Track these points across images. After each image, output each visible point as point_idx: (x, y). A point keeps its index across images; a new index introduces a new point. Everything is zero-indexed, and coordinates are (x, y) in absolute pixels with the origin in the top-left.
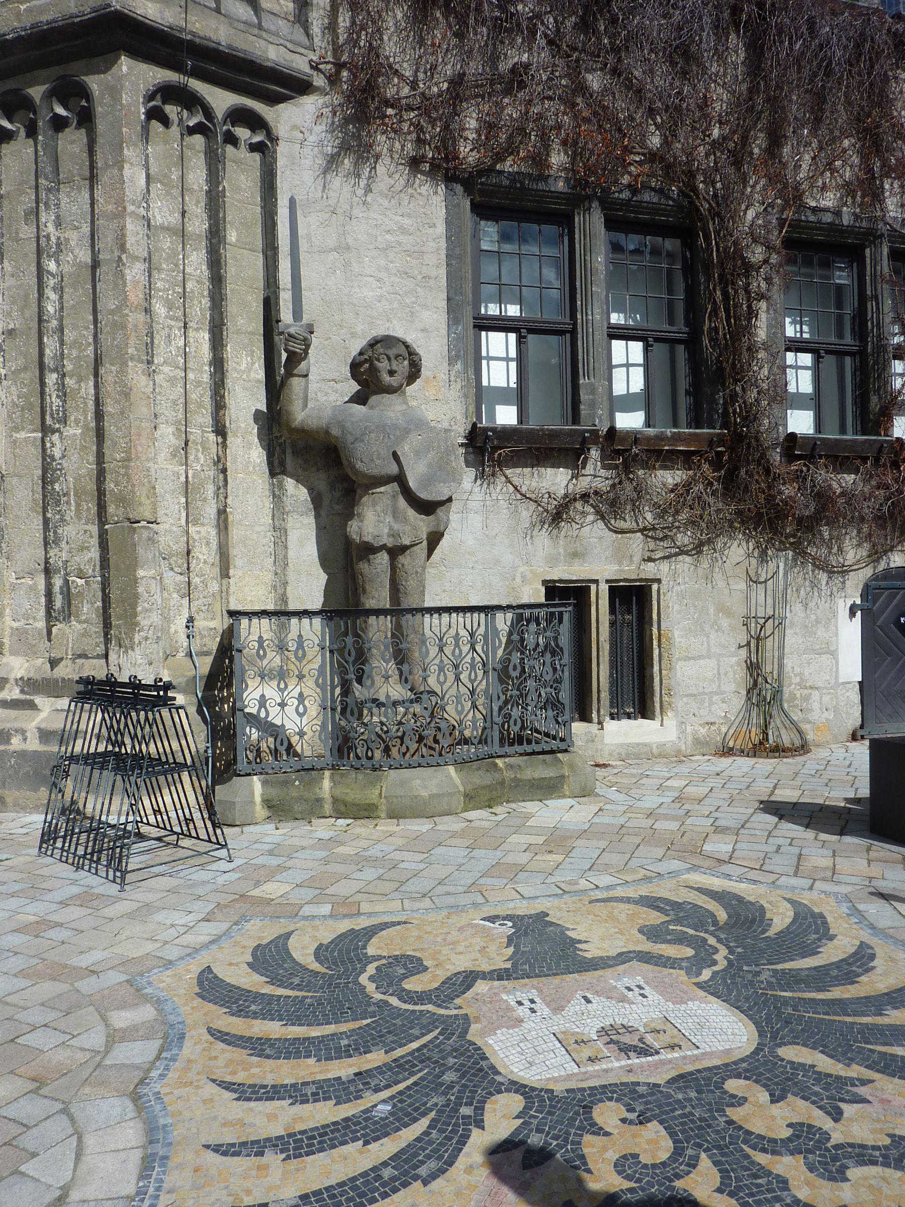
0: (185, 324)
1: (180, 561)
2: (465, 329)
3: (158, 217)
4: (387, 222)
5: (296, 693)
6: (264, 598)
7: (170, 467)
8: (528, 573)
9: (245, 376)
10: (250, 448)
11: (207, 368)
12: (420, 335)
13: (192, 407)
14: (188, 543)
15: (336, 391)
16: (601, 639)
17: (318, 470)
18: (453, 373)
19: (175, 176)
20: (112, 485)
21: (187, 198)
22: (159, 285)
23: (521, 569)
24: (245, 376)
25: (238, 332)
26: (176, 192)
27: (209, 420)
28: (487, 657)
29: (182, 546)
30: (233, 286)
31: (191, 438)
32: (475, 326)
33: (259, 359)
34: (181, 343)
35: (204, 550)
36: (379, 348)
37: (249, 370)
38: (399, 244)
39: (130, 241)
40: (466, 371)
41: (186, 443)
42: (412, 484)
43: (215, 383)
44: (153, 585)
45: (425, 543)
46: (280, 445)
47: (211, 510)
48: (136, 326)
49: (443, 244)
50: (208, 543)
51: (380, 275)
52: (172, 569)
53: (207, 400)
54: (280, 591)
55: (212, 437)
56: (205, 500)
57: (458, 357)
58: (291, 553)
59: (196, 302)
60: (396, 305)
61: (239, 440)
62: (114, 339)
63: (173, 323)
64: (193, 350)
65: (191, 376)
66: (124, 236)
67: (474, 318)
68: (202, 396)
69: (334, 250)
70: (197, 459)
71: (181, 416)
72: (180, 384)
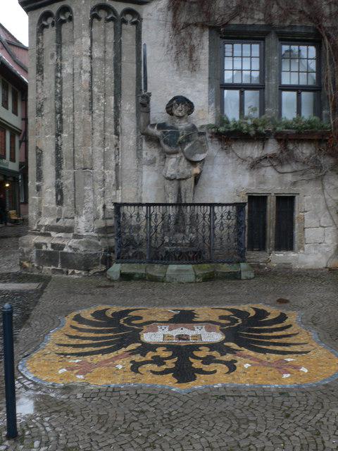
12: (197, 93)
19: (102, 38)
26: (102, 45)
27: (113, 130)
39: (84, 65)
47: (113, 164)
53: (112, 122)
55: (114, 136)
58: (144, 181)
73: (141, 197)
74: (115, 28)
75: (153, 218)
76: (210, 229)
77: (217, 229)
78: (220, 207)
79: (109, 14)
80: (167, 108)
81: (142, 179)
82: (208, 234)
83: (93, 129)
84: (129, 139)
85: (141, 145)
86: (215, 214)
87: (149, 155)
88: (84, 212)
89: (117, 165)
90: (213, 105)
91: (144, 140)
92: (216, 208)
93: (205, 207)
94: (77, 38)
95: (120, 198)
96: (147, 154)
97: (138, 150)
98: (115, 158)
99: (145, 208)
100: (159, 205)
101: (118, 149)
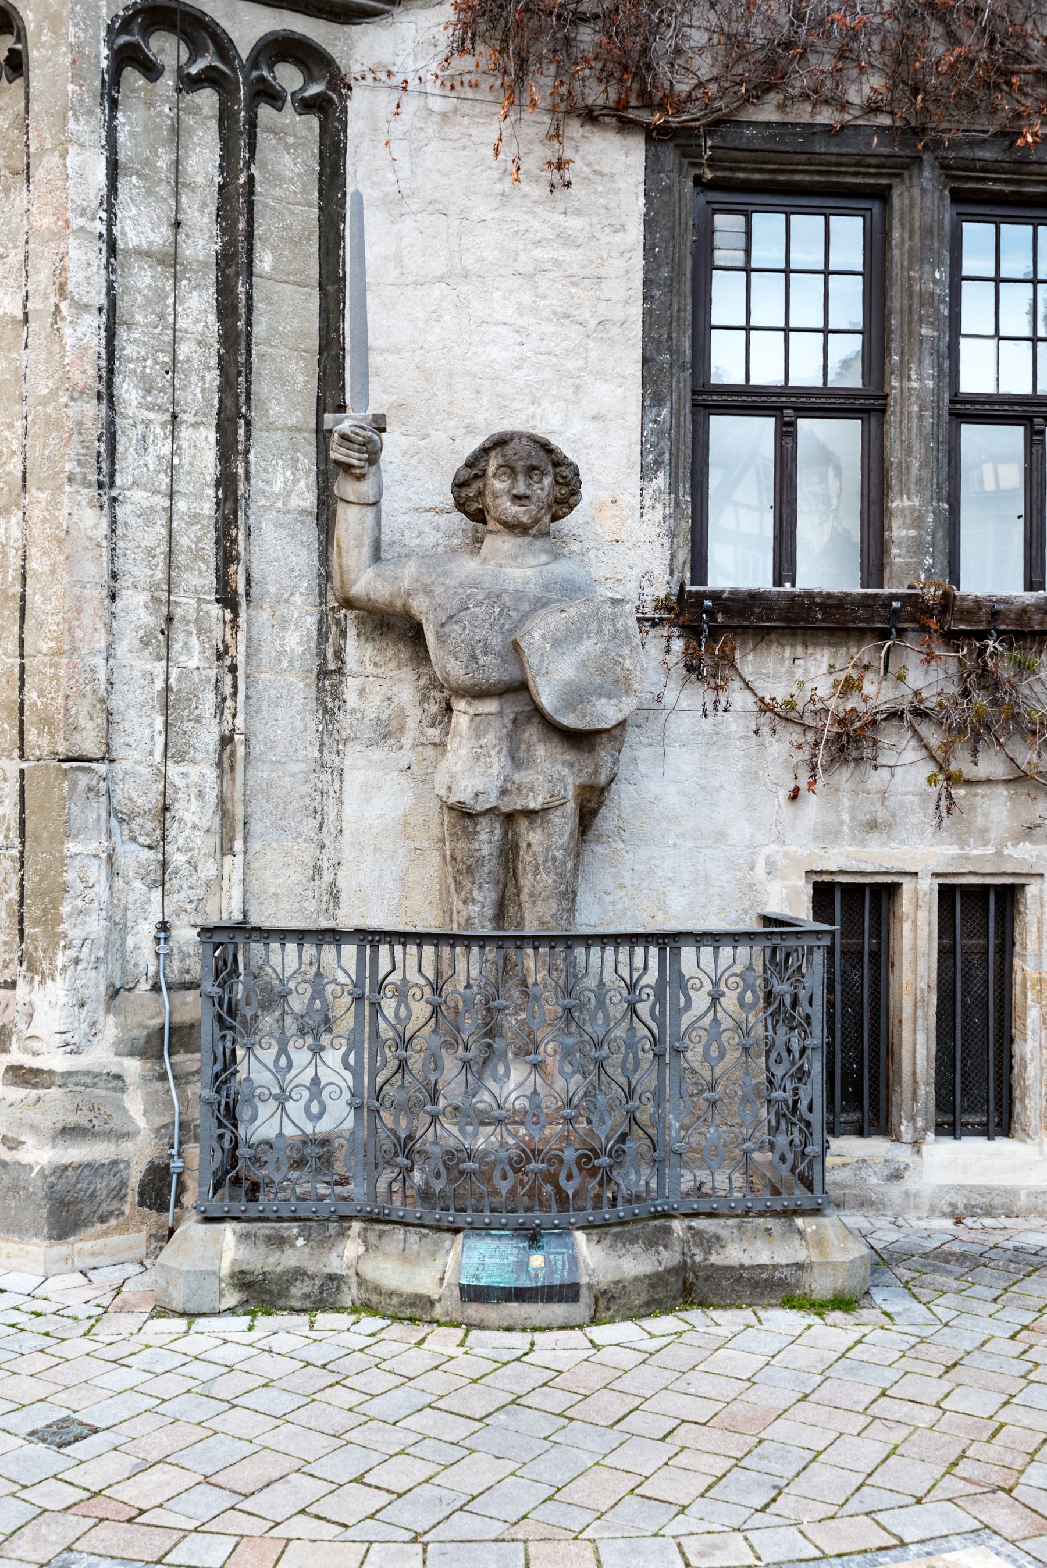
0: (174, 417)
1: (149, 826)
3: (131, 234)
4: (536, 224)
5: (307, 1077)
6: (299, 890)
7: (137, 664)
8: (779, 858)
9: (279, 504)
10: (284, 629)
11: (211, 492)
12: (590, 426)
13: (181, 559)
17: (399, 667)
18: (648, 493)
19: (163, 162)
20: (34, 695)
21: (184, 199)
22: (130, 350)
23: (766, 851)
25: (270, 427)
26: (164, 190)
27: (210, 581)
28: (661, 1026)
31: (178, 612)
33: (307, 473)
34: (166, 450)
35: (195, 805)
37: (288, 494)
38: (557, 263)
39: (75, 278)
40: (673, 488)
41: (170, 619)
42: (547, 699)
43: (225, 518)
44: (94, 869)
45: (571, 807)
46: (338, 622)
47: (208, 737)
48: (80, 424)
49: (638, 261)
50: (200, 795)
51: (521, 322)
52: (134, 839)
54: (328, 877)
55: (215, 610)
56: (198, 720)
57: (658, 463)
58: (348, 811)
59: (194, 379)
60: (548, 374)
62: (45, 446)
63: (152, 415)
64: (186, 461)
65: (181, 505)
66: (64, 269)
67: (694, 392)
68: (200, 539)
69: (441, 279)
71: (160, 575)
72: (162, 520)
73: (333, 884)
74: (225, 117)
75: (389, 1006)
79: (195, 53)
80: (459, 485)
81: (340, 802)
83: (114, 575)
84: (284, 624)
85: (339, 655)
87: (375, 700)
88: (61, 959)
89: (226, 740)
90: (661, 480)
91: (351, 632)
93: (639, 951)
94: (42, 151)
95: (237, 892)
96: (362, 692)
97: (323, 673)
98: (220, 709)
99: (349, 950)
100: (420, 938)
101: (233, 669)
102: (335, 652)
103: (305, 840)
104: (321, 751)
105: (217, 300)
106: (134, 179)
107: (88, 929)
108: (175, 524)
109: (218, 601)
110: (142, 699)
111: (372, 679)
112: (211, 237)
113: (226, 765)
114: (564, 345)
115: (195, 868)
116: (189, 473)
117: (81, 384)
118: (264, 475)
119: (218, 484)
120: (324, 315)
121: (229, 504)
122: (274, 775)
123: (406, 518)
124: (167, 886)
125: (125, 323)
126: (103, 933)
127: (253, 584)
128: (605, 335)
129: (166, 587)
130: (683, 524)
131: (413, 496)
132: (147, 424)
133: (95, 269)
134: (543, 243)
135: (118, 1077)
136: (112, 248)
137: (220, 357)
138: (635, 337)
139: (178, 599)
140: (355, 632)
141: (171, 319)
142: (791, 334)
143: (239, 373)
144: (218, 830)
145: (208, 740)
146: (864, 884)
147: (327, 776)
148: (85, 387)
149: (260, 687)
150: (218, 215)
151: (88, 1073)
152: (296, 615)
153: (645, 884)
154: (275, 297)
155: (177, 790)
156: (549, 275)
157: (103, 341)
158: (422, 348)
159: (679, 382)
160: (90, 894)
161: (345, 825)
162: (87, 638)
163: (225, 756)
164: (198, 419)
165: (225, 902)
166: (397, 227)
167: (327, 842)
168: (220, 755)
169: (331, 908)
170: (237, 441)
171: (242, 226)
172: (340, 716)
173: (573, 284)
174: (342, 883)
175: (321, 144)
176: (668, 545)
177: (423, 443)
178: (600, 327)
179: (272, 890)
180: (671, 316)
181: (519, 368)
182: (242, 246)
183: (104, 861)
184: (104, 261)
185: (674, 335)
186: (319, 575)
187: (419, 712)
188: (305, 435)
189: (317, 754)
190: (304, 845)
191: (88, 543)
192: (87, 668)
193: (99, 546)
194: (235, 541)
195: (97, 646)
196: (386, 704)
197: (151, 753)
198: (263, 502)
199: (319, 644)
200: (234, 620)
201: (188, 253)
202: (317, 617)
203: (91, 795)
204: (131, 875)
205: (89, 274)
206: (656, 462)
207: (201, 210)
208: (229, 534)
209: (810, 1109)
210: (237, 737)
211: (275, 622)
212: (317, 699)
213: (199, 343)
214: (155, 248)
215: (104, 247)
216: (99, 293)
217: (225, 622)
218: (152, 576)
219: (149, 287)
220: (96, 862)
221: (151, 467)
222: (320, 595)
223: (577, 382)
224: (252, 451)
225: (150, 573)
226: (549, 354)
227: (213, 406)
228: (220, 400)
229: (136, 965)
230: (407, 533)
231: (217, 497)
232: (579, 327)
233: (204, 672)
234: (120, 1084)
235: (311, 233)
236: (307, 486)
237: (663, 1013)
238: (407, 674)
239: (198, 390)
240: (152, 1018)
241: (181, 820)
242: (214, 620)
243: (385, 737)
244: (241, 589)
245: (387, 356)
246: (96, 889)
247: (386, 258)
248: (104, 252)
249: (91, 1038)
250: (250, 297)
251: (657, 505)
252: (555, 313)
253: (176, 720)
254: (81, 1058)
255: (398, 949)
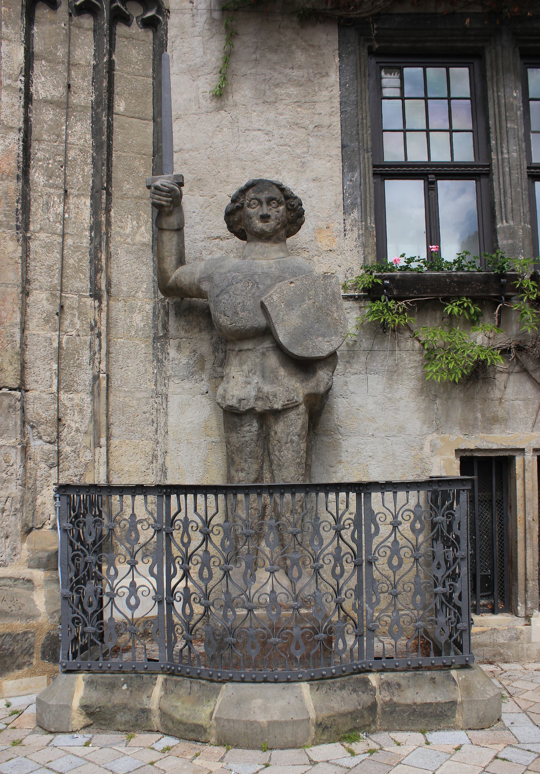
0: (66, 191)
1: (49, 430)
2: (363, 176)
3: (41, 92)
7: (42, 333)
11: (87, 233)
12: (312, 185)
13: (69, 272)
14: (58, 410)
15: (221, 249)
16: (529, 518)
17: (200, 331)
19: (61, 53)
21: (73, 73)
24: (129, 240)
26: (61, 68)
27: (86, 284)
29: (52, 414)
30: (119, 153)
31: (67, 303)
32: (375, 174)
33: (146, 223)
34: (60, 210)
35: (77, 417)
36: (251, 194)
43: (95, 248)
44: (13, 455)
50: (81, 411)
51: (269, 128)
52: (40, 438)
53: (86, 264)
54: (160, 461)
55: (90, 301)
56: (79, 366)
57: (353, 205)
61: (120, 304)
63: (52, 191)
64: (73, 216)
65: (69, 241)
68: (80, 260)
70: (72, 324)
71: (56, 281)
72: (58, 250)
73: (163, 464)
75: (177, 535)
76: (358, 566)
77: (382, 564)
78: (389, 495)
81: (166, 414)
82: (353, 582)
84: (132, 310)
86: (372, 516)
90: (356, 214)
91: (172, 313)
92: (376, 496)
93: (342, 495)
95: (103, 470)
97: (156, 338)
98: (92, 359)
101: (99, 335)
102: (163, 325)
103: (147, 439)
104: (156, 385)
105: (92, 127)
106: (43, 62)
107: (9, 491)
108: (65, 252)
109: (91, 296)
110: (45, 354)
111: (184, 340)
112: (88, 93)
113: (96, 393)
114: (294, 140)
115: (78, 455)
116: (74, 223)
117: (7, 171)
118: (119, 223)
119: (91, 229)
120: (156, 135)
121: (98, 239)
122: (127, 399)
123: (203, 244)
124: (61, 466)
125: (36, 140)
126: (19, 494)
127: (113, 286)
128: (319, 134)
129: (59, 288)
130: (371, 240)
131: (207, 231)
132: (49, 195)
133: (17, 108)
134: (281, 85)
135: (29, 581)
136: (28, 98)
137: (93, 158)
138: (336, 134)
139: (67, 295)
140: (174, 312)
141: (64, 137)
142: (431, 133)
143: (103, 164)
144: (92, 432)
145: (85, 378)
146: (491, 457)
147: (158, 400)
148: (10, 172)
149: (118, 347)
150: (93, 82)
151: (10, 578)
152: (139, 304)
153: (355, 460)
154: (127, 125)
155: (66, 408)
156: (284, 102)
157: (21, 147)
158: (211, 147)
159: (364, 158)
160: (11, 469)
161: (169, 429)
162: (9, 316)
163: (95, 388)
164: (80, 193)
165: (96, 476)
166: (196, 83)
167: (160, 440)
168: (93, 387)
169: (162, 479)
170: (101, 203)
171: (105, 84)
172: (166, 363)
173: (299, 106)
174: (168, 464)
175: (154, 44)
176: (362, 252)
177: (212, 200)
178: (316, 129)
179: (126, 469)
180: (358, 121)
181: (267, 154)
182: (105, 95)
183: (19, 450)
184: (22, 103)
185: (360, 132)
186: (154, 281)
187: (212, 358)
188: (145, 201)
189: (154, 387)
190: (146, 442)
191: (10, 261)
192: (9, 334)
193: (17, 263)
194: (100, 260)
195: (15, 321)
196: (192, 354)
197: (51, 386)
198: (119, 239)
199: (154, 321)
200: (100, 306)
201: (75, 101)
202: (152, 305)
203: (11, 410)
204: (39, 459)
205: (13, 110)
206: (352, 204)
207: (83, 79)
208: (97, 256)
209: (460, 597)
210: (101, 375)
211: (126, 309)
212: (153, 354)
213: (81, 150)
214: (56, 99)
215: (23, 96)
216: (19, 121)
217: (95, 308)
218: (51, 282)
219: (51, 120)
220: (14, 450)
221: (51, 219)
222: (154, 293)
223: (303, 160)
224: (112, 210)
225: (50, 280)
226: (286, 145)
227: (89, 185)
228: (93, 182)
229: (43, 514)
230: (204, 252)
231: (91, 236)
232: (303, 130)
233: (83, 338)
234: (31, 586)
235: (149, 91)
236: (146, 229)
237: (360, 537)
238: (205, 336)
239: (80, 176)
240: (51, 545)
241: (69, 426)
242: (89, 307)
243: (192, 374)
244: (103, 287)
245: (191, 153)
246: (15, 467)
247: (190, 100)
248: (22, 99)
249: (12, 557)
250: (110, 126)
251: (354, 229)
252: (288, 122)
253: (65, 366)
254: (7, 569)
255: (182, 497)
